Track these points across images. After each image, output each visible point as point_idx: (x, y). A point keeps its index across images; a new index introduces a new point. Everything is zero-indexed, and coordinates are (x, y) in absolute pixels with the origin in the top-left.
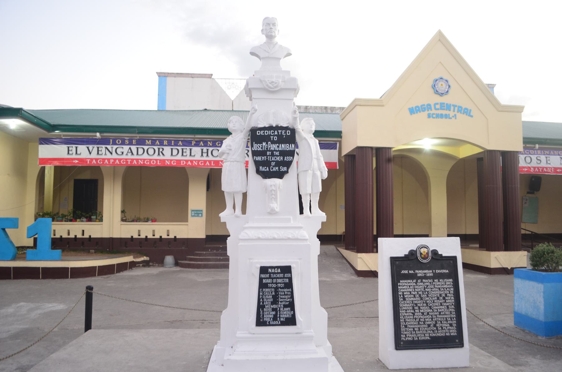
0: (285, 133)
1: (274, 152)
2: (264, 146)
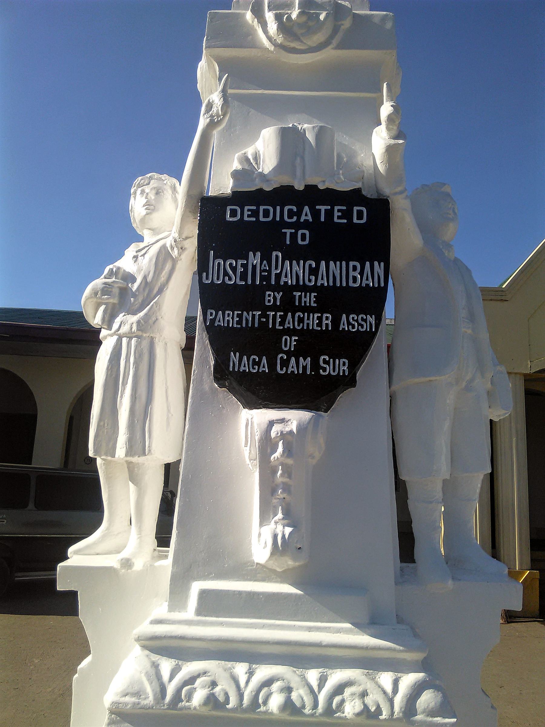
0: (347, 214)
2: (254, 267)
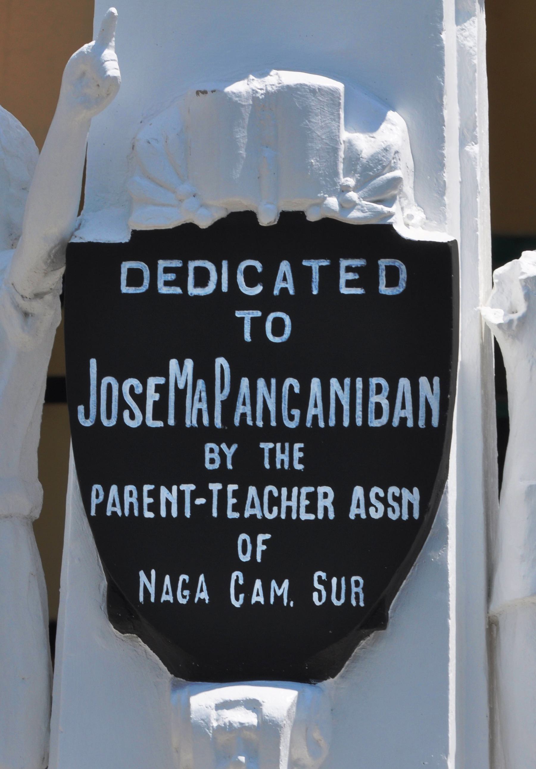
1: (266, 446)
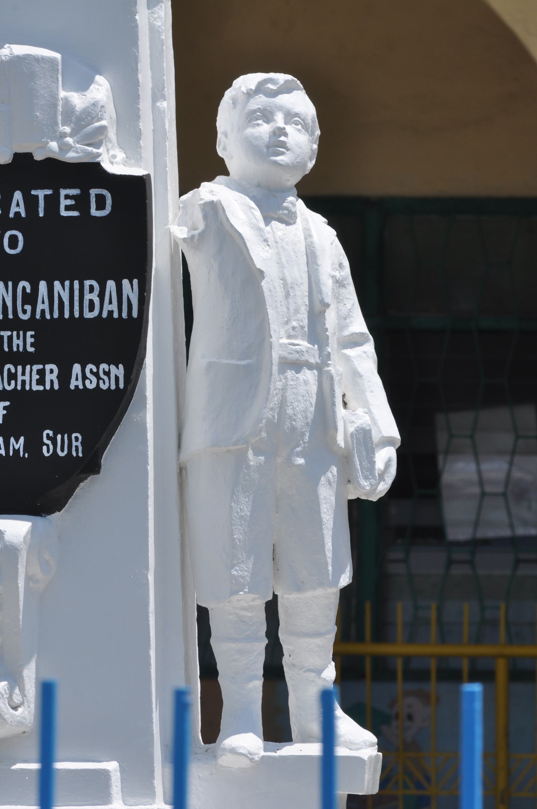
1: (6, 334)
